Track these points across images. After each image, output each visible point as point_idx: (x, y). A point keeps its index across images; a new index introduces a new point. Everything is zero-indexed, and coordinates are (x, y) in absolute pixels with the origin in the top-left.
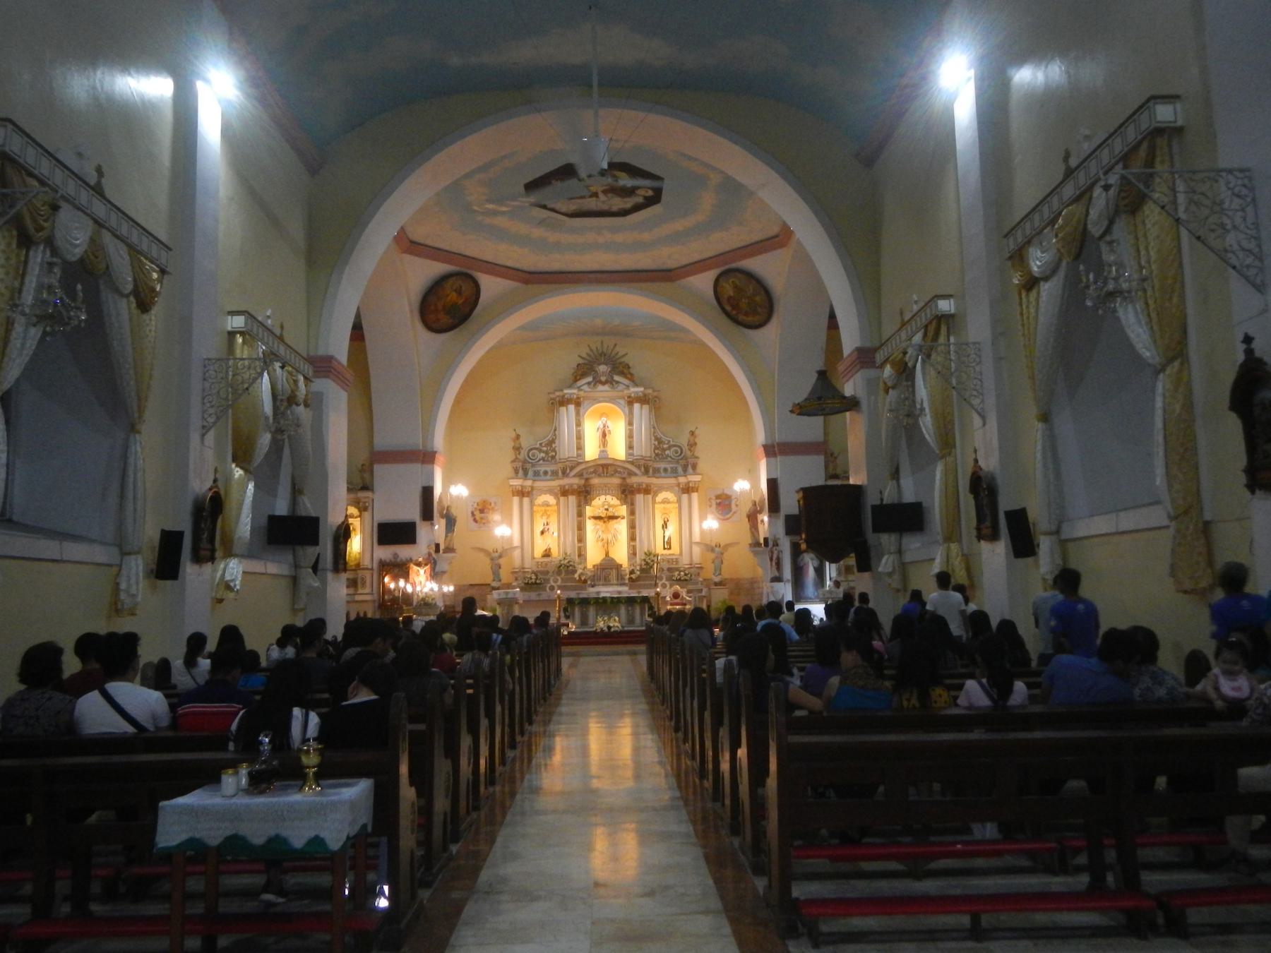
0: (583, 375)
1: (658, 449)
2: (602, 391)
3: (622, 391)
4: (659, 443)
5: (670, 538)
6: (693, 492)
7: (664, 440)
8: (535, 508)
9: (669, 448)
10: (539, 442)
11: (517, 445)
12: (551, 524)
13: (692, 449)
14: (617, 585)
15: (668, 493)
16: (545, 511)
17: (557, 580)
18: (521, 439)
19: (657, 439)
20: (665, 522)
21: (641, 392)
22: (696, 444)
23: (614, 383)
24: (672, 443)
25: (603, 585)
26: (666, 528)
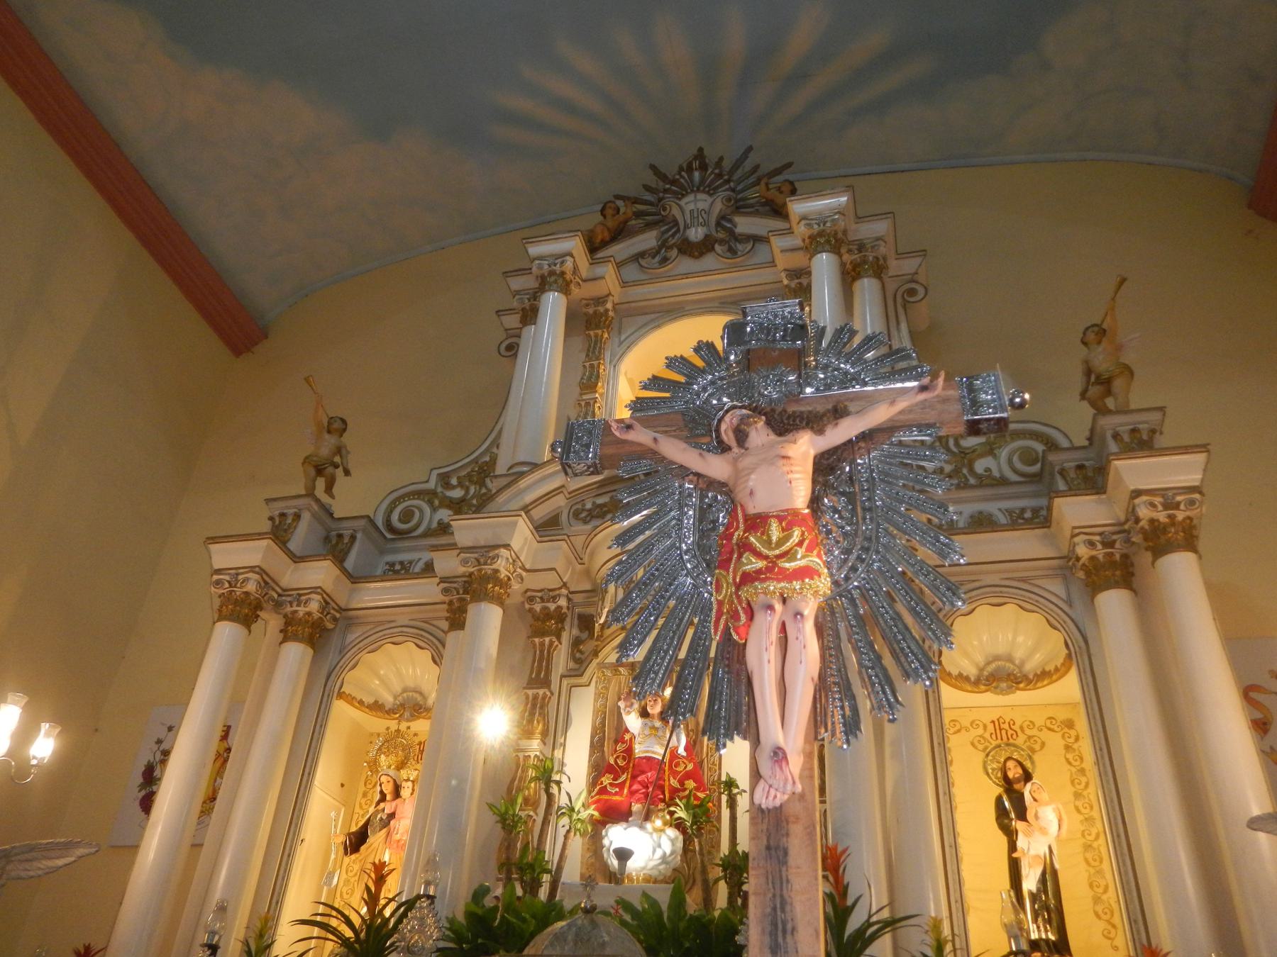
0: (618, 234)
2: (686, 275)
3: (773, 263)
5: (1050, 877)
6: (1159, 551)
10: (435, 472)
11: (325, 451)
12: (405, 793)
13: (1110, 403)
15: (1010, 610)
16: (391, 741)
18: (347, 439)
20: (1008, 784)
22: (1128, 371)
23: (740, 247)
26: (1022, 816)
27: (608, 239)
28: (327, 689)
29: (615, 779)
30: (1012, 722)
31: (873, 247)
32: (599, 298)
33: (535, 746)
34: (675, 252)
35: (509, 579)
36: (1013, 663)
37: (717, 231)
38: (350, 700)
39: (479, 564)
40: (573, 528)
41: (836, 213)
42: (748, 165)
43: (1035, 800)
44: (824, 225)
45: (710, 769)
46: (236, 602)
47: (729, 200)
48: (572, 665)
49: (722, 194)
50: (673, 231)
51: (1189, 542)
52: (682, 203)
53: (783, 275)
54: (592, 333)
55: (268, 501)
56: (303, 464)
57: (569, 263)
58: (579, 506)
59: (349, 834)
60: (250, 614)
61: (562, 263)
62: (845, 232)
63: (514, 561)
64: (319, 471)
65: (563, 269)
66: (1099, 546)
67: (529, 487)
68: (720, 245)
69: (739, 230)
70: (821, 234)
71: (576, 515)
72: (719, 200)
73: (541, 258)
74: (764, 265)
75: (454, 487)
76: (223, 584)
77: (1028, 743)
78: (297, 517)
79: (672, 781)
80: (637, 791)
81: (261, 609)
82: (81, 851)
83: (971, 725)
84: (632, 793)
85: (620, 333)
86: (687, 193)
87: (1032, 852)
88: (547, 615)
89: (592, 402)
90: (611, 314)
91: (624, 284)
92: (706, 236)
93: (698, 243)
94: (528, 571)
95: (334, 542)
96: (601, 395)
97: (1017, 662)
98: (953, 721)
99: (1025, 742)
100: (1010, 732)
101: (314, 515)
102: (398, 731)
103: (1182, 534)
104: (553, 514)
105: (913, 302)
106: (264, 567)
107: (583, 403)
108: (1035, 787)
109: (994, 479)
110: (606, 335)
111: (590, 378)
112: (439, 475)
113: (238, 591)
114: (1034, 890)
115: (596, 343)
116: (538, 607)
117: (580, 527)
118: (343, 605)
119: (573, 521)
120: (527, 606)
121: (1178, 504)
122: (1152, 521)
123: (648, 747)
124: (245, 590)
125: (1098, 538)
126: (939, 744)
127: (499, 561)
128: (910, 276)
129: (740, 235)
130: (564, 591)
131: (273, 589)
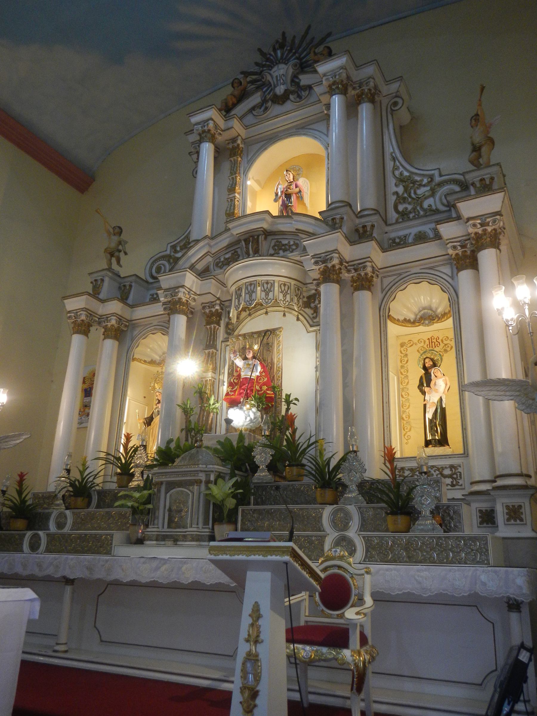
0: (241, 98)
1: (404, 200)
2: (277, 116)
3: (319, 101)
4: (406, 189)
7: (418, 178)
8: (135, 366)
9: (433, 193)
11: (113, 245)
14: (198, 538)
15: (425, 284)
17: (66, 517)
18: (123, 237)
19: (401, 180)
21: (342, 68)
22: (492, 141)
23: (303, 93)
24: (437, 179)
25: (162, 538)
26: (428, 385)
27: (236, 102)
28: (128, 357)
29: (232, 389)
30: (438, 338)
31: (367, 83)
32: (234, 138)
33: (210, 375)
34: (270, 103)
35: (187, 301)
36: (431, 309)
37: (291, 85)
38: (139, 360)
39: (173, 296)
40: (216, 272)
41: (340, 70)
42: (309, 37)
43: (436, 377)
44: (335, 77)
45: (278, 379)
46: (79, 325)
47: (295, 65)
48: (226, 336)
49: (293, 62)
50: (270, 90)
51: (495, 243)
52: (272, 72)
53: (324, 108)
54: (232, 159)
55: (90, 274)
56: (104, 252)
57: (211, 124)
58: (218, 260)
59: (145, 419)
60: (86, 329)
61: (207, 125)
62: (348, 78)
63: (189, 292)
64: (112, 255)
65: (208, 128)
66: (459, 248)
67: (193, 255)
68: (292, 95)
69: (302, 83)
70: (334, 83)
71: (217, 265)
72: (290, 67)
73: (198, 124)
74: (315, 103)
75: (178, 252)
76: (72, 317)
77: (445, 348)
78: (102, 280)
79: (257, 386)
80: (242, 393)
81: (92, 326)
82: (24, 437)
83: (418, 342)
84: (240, 394)
85: (247, 156)
86: (274, 65)
87: (431, 401)
88: (212, 314)
89: (233, 199)
90: (241, 146)
91: (246, 127)
92: (286, 90)
93: (282, 95)
94: (199, 295)
95: (123, 289)
96: (239, 193)
97: (434, 310)
98: (409, 341)
99: (443, 347)
100: (436, 343)
101: (111, 278)
102: (162, 372)
103: (489, 239)
104: (206, 267)
105: (397, 110)
106: (87, 307)
107: (229, 200)
108: (435, 371)
109: (434, 211)
110: (239, 159)
111: (232, 185)
112: (171, 246)
113: (79, 320)
114: (431, 418)
115: (235, 165)
116: (207, 311)
117: (219, 271)
118: (129, 318)
119: (215, 268)
120: (203, 311)
121: (489, 223)
122: (476, 233)
123: (245, 374)
124: (81, 319)
125: (459, 244)
126: (385, 356)
127: (180, 294)
128: (394, 94)
129: (304, 86)
130: (218, 302)
131: (95, 317)
